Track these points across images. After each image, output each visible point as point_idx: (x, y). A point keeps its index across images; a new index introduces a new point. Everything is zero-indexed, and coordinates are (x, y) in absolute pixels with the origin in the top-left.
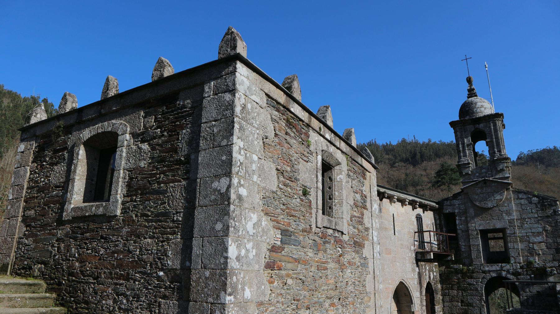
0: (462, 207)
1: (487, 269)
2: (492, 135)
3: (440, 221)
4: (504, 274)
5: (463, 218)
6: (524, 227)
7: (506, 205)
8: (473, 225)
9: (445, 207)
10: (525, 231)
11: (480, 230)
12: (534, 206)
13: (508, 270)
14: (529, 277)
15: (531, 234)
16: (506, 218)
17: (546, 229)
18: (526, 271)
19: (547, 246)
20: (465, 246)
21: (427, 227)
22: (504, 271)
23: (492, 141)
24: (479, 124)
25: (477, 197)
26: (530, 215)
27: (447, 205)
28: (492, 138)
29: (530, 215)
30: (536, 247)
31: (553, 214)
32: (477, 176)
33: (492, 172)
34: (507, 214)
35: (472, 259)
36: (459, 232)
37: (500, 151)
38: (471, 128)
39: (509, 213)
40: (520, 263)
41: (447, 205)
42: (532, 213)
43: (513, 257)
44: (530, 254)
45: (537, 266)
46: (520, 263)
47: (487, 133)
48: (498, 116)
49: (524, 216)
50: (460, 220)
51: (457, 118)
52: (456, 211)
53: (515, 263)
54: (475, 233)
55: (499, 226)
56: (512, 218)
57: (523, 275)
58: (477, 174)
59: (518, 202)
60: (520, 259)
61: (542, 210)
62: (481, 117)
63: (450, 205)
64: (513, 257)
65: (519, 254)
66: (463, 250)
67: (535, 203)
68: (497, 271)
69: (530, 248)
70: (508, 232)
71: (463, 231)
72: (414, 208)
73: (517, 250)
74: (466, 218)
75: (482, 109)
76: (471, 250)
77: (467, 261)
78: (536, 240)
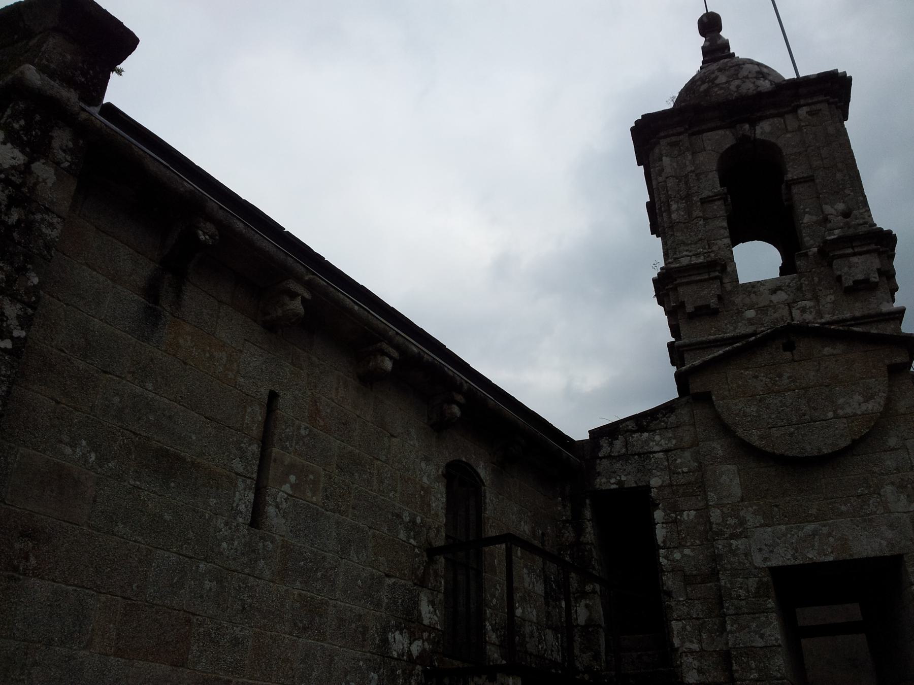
0: (685, 461)
9: (603, 465)
11: (775, 571)
20: (701, 654)
24: (753, 124)
25: (753, 410)
27: (609, 457)
32: (750, 322)
33: (816, 298)
36: (669, 581)
38: (717, 141)
50: (675, 521)
52: (655, 482)
54: (752, 583)
55: (867, 544)
58: (751, 314)
71: (688, 580)
72: (439, 427)
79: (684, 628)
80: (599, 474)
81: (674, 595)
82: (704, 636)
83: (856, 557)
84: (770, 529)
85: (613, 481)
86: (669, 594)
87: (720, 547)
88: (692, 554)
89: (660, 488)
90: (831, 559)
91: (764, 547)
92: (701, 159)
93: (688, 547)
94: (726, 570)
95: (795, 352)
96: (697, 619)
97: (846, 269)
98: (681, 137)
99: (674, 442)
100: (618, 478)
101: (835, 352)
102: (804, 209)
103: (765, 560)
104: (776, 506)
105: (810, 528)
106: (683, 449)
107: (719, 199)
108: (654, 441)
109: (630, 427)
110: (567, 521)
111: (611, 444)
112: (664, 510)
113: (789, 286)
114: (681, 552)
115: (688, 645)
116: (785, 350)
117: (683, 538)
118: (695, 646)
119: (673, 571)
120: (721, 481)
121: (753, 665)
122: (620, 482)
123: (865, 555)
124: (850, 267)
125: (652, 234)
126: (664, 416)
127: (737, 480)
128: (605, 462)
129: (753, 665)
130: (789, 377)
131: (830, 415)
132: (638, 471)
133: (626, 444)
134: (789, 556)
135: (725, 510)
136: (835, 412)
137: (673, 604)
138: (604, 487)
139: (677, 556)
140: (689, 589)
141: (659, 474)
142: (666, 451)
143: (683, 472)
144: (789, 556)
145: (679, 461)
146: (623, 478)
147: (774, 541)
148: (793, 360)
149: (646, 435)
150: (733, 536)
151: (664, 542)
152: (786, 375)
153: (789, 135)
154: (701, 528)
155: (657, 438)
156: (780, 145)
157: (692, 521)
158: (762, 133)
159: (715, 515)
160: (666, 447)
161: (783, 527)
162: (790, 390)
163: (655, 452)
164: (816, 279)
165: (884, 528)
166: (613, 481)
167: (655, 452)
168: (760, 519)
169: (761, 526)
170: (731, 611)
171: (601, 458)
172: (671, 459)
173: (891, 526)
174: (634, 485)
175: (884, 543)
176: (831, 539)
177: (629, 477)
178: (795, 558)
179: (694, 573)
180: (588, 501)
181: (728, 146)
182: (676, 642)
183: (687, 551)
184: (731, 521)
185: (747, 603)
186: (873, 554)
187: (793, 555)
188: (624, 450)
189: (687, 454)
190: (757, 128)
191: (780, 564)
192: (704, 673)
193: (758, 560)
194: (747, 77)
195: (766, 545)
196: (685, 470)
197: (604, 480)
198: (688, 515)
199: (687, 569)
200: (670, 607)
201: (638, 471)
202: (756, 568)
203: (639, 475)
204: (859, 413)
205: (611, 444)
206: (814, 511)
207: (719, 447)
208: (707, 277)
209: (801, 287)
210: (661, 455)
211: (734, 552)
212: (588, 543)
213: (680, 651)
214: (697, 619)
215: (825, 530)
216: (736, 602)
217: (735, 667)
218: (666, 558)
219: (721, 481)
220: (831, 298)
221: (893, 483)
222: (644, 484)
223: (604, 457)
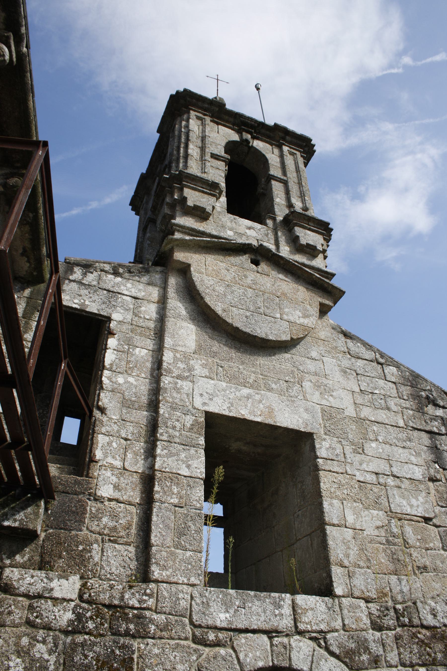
1: (221, 618)
7: (314, 354)
8: (186, 385)
10: (372, 467)
15: (390, 481)
22: (300, 633)
24: (254, 138)
26: (382, 416)
29: (382, 416)
41: (80, 283)
42: (388, 409)
49: (366, 412)
54: (189, 420)
55: (288, 417)
66: (105, 491)
68: (271, 633)
78: (409, 510)
79: (109, 444)
81: (108, 412)
83: (278, 424)
84: (212, 382)
85: (76, 301)
86: (102, 410)
87: (166, 382)
88: (135, 383)
90: (259, 419)
91: (205, 394)
94: (167, 402)
96: (126, 439)
97: (303, 234)
99: (143, 294)
100: (82, 301)
103: (204, 404)
104: (221, 367)
105: (246, 391)
106: (149, 301)
109: (106, 269)
111: (84, 275)
112: (119, 340)
115: (110, 460)
117: (130, 368)
118: (118, 463)
119: (112, 391)
121: (175, 491)
122: (83, 304)
127: (194, 337)
128: (74, 286)
129: (175, 491)
131: (278, 316)
134: (225, 408)
135: (178, 355)
137: (105, 419)
139: (121, 380)
141: (122, 311)
143: (145, 318)
144: (225, 408)
145: (143, 309)
146: (87, 303)
150: (179, 377)
151: (111, 365)
152: (250, 278)
155: (129, 285)
157: (142, 357)
160: (134, 295)
161: (224, 384)
162: (251, 288)
163: (124, 295)
165: (302, 410)
166: (76, 301)
167: (124, 295)
168: (206, 372)
169: (206, 377)
170: (165, 437)
171: (71, 281)
173: (306, 410)
174: (96, 312)
175: (301, 421)
176: (261, 406)
177: (94, 304)
179: (133, 399)
182: (99, 454)
183: (131, 380)
184: (181, 365)
185: (181, 434)
186: (291, 427)
187: (229, 408)
192: (119, 490)
193: (198, 403)
195: (207, 393)
198: (140, 352)
199: (126, 393)
200: (102, 422)
202: (195, 408)
204: (298, 322)
205: (84, 275)
206: (251, 381)
211: (178, 390)
214: (126, 439)
215: (257, 397)
216: (171, 431)
218: (109, 378)
219: (180, 333)
222: (105, 314)
223: (74, 281)
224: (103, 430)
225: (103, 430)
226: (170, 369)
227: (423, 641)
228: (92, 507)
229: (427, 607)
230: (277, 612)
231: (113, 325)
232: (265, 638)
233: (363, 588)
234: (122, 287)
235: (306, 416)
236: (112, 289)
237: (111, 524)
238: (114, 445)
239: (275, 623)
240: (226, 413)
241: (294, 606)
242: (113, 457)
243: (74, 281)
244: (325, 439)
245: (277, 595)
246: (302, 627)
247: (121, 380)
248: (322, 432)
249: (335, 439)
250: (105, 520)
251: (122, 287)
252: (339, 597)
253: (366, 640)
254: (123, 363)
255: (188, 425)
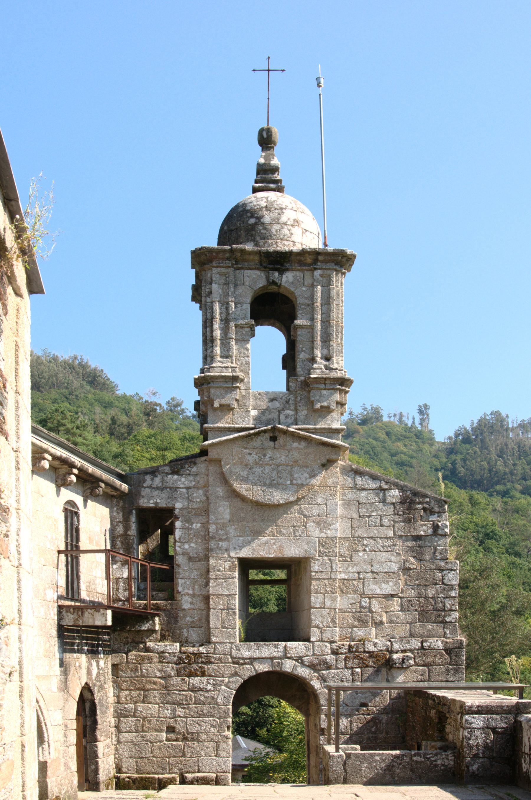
0: (198, 495)
2: (313, 310)
3: (127, 528)
4: (288, 666)
5: (197, 526)
6: (356, 559)
7: (319, 501)
9: (145, 492)
12: (391, 510)
13: (301, 658)
14: (348, 673)
16: (315, 532)
17: (407, 565)
18: (345, 659)
19: (402, 605)
20: (193, 596)
21: (90, 540)
22: (289, 658)
23: (312, 328)
24: (282, 272)
27: (151, 487)
28: (312, 319)
30: (376, 606)
31: (430, 531)
33: (296, 410)
34: (318, 524)
35: (209, 628)
36: (180, 560)
37: (328, 359)
38: (254, 279)
39: (323, 523)
40: (331, 642)
41: (151, 487)
43: (317, 627)
44: (360, 620)
45: (371, 648)
46: (331, 642)
47: (300, 300)
48: (341, 260)
51: (212, 242)
52: (178, 505)
53: (322, 640)
56: (330, 533)
57: (337, 668)
59: (351, 495)
60: (333, 632)
61: (408, 521)
62: (291, 253)
63: (161, 489)
64: (317, 627)
65: (333, 621)
66: (186, 606)
67: (393, 504)
68: (272, 659)
69: (361, 607)
70: (315, 567)
71: (190, 559)
73: (328, 610)
74: (205, 526)
75: (296, 231)
76: (208, 608)
77: (194, 635)
79: (185, 583)
80: (143, 497)
81: (182, 566)
82: (196, 587)
83: (285, 556)
84: (242, 538)
85: (151, 501)
86: (179, 566)
88: (195, 546)
89: (181, 509)
90: (272, 556)
92: (240, 291)
93: (194, 543)
95: (276, 442)
96: (194, 579)
98: (229, 270)
99: (193, 483)
100: (155, 500)
101: (300, 446)
102: (302, 348)
107: (247, 327)
108: (180, 481)
109: (166, 471)
110: (120, 522)
111: (152, 480)
112: (182, 522)
113: (281, 399)
114: (189, 545)
116: (270, 440)
117: (191, 538)
118: (191, 592)
119: (183, 554)
120: (219, 510)
121: (221, 603)
122: (156, 503)
123: (291, 556)
124: (320, 396)
125: (193, 300)
126: (189, 467)
128: (148, 490)
130: (270, 457)
132: (169, 498)
133: (163, 481)
134: (250, 553)
136: (291, 481)
137: (180, 570)
138: (145, 505)
139: (186, 546)
140: (191, 564)
141: (181, 501)
142: (188, 488)
143: (197, 502)
144: (250, 553)
145: (195, 495)
146: (158, 501)
147: (243, 544)
148: (275, 448)
149: (176, 477)
151: (180, 539)
153: (304, 289)
154: (202, 533)
155: (183, 479)
156: (296, 294)
157: (198, 529)
158: (286, 282)
159: (212, 528)
160: (187, 485)
163: (181, 488)
164: (299, 398)
167: (181, 488)
171: (145, 488)
172: (190, 493)
173: (308, 543)
174: (165, 506)
176: (275, 547)
177: (163, 501)
178: (253, 554)
179: (195, 556)
180: (134, 512)
181: (261, 285)
182: (180, 589)
183: (193, 545)
188: (160, 484)
189: (201, 492)
190: (284, 276)
191: (244, 556)
192: (193, 605)
194: (285, 224)
195: (238, 546)
196: (198, 500)
197: (146, 501)
198: (196, 526)
199: (191, 554)
200: (179, 572)
201: (169, 498)
203: (169, 500)
205: (152, 480)
207: (221, 490)
208: (230, 385)
209: (289, 401)
210: (184, 490)
212: (132, 536)
213: (182, 593)
215: (272, 541)
217: (211, 603)
218: (180, 547)
220: (305, 412)
221: (314, 522)
222: (171, 506)
223: (147, 487)
224: (181, 576)
225: (181, 576)
226: (214, 536)
227: (362, 658)
228: (181, 614)
229: (372, 643)
230: (276, 650)
231: (177, 512)
232: (269, 660)
233: (329, 637)
234: (179, 483)
235: (306, 547)
236: (172, 486)
237: (191, 620)
238: (188, 583)
239: (275, 654)
240: (250, 556)
241: (285, 647)
242: (188, 589)
243: (147, 487)
244: (318, 560)
245: (276, 643)
246: (289, 655)
247: (186, 546)
248: (317, 555)
249: (326, 558)
250: (188, 618)
251: (179, 483)
252: (313, 642)
253: (326, 659)
254: (187, 536)
255: (227, 567)
